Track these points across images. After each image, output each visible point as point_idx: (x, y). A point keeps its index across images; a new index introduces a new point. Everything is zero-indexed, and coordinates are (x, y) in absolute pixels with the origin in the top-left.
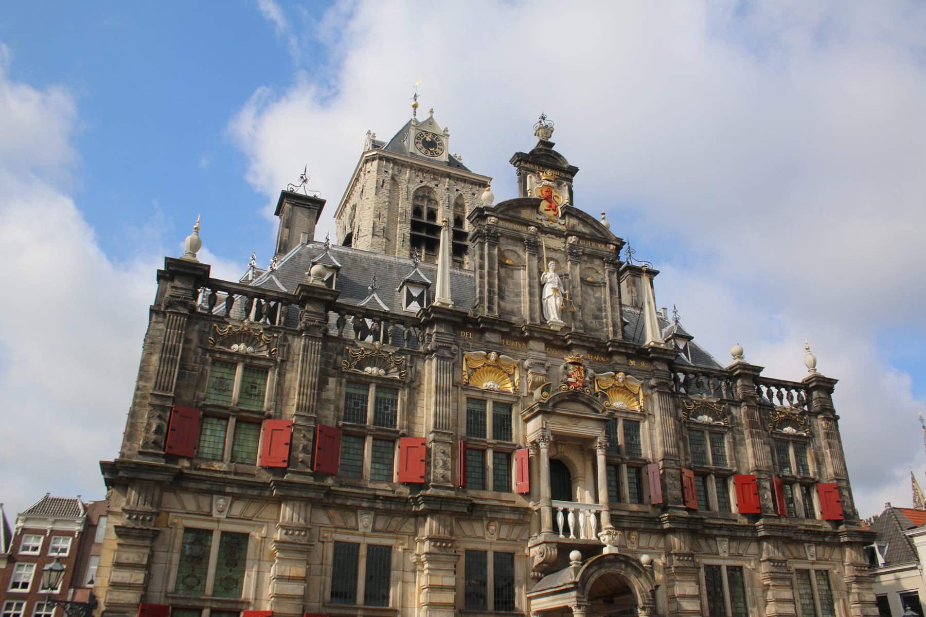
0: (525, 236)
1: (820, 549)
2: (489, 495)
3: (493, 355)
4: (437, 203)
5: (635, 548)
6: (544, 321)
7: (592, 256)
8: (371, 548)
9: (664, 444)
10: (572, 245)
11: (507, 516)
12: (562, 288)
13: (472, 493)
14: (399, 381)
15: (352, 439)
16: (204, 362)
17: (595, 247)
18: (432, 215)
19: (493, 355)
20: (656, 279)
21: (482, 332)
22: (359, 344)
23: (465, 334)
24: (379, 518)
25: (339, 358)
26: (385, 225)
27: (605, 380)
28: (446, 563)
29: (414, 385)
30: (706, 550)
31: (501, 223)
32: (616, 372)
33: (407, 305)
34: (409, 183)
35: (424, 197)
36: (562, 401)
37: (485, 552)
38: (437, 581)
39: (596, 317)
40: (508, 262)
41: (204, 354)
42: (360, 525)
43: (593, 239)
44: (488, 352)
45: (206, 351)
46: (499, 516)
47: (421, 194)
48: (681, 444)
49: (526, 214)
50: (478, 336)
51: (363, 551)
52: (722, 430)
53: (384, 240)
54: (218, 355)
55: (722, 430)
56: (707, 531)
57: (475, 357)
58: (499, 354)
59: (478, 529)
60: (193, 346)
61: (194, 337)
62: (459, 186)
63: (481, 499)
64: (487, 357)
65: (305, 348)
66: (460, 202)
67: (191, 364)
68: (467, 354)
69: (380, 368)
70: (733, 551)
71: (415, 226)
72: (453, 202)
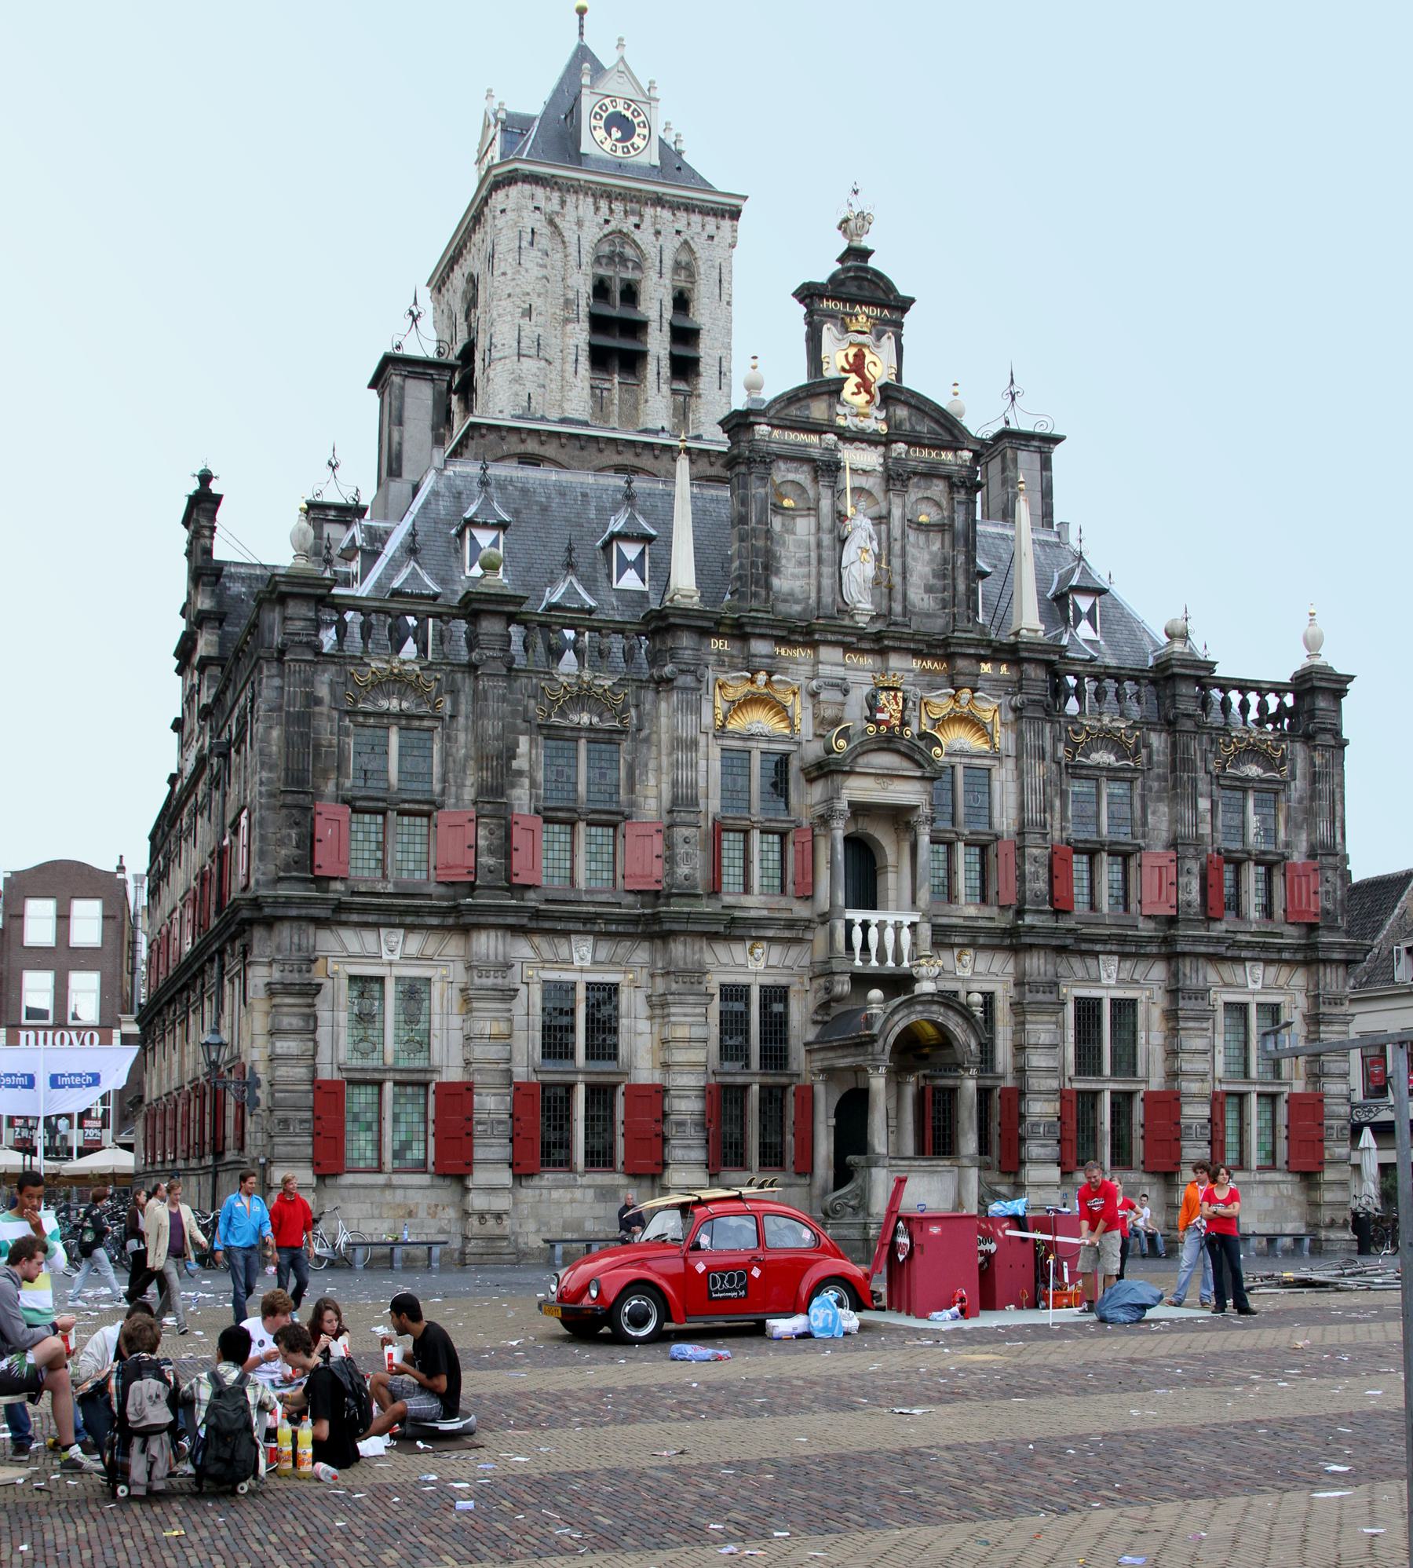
1: (1272, 970)
2: (756, 904)
3: (762, 677)
4: (638, 266)
6: (846, 610)
8: (590, 986)
15: (557, 827)
18: (630, 294)
19: (762, 677)
24: (600, 944)
29: (643, 734)
30: (1081, 973)
37: (748, 987)
42: (576, 957)
47: (606, 249)
51: (581, 993)
56: (1084, 946)
58: (770, 674)
59: (738, 952)
64: (752, 681)
66: (684, 258)
71: (598, 323)
72: (668, 263)
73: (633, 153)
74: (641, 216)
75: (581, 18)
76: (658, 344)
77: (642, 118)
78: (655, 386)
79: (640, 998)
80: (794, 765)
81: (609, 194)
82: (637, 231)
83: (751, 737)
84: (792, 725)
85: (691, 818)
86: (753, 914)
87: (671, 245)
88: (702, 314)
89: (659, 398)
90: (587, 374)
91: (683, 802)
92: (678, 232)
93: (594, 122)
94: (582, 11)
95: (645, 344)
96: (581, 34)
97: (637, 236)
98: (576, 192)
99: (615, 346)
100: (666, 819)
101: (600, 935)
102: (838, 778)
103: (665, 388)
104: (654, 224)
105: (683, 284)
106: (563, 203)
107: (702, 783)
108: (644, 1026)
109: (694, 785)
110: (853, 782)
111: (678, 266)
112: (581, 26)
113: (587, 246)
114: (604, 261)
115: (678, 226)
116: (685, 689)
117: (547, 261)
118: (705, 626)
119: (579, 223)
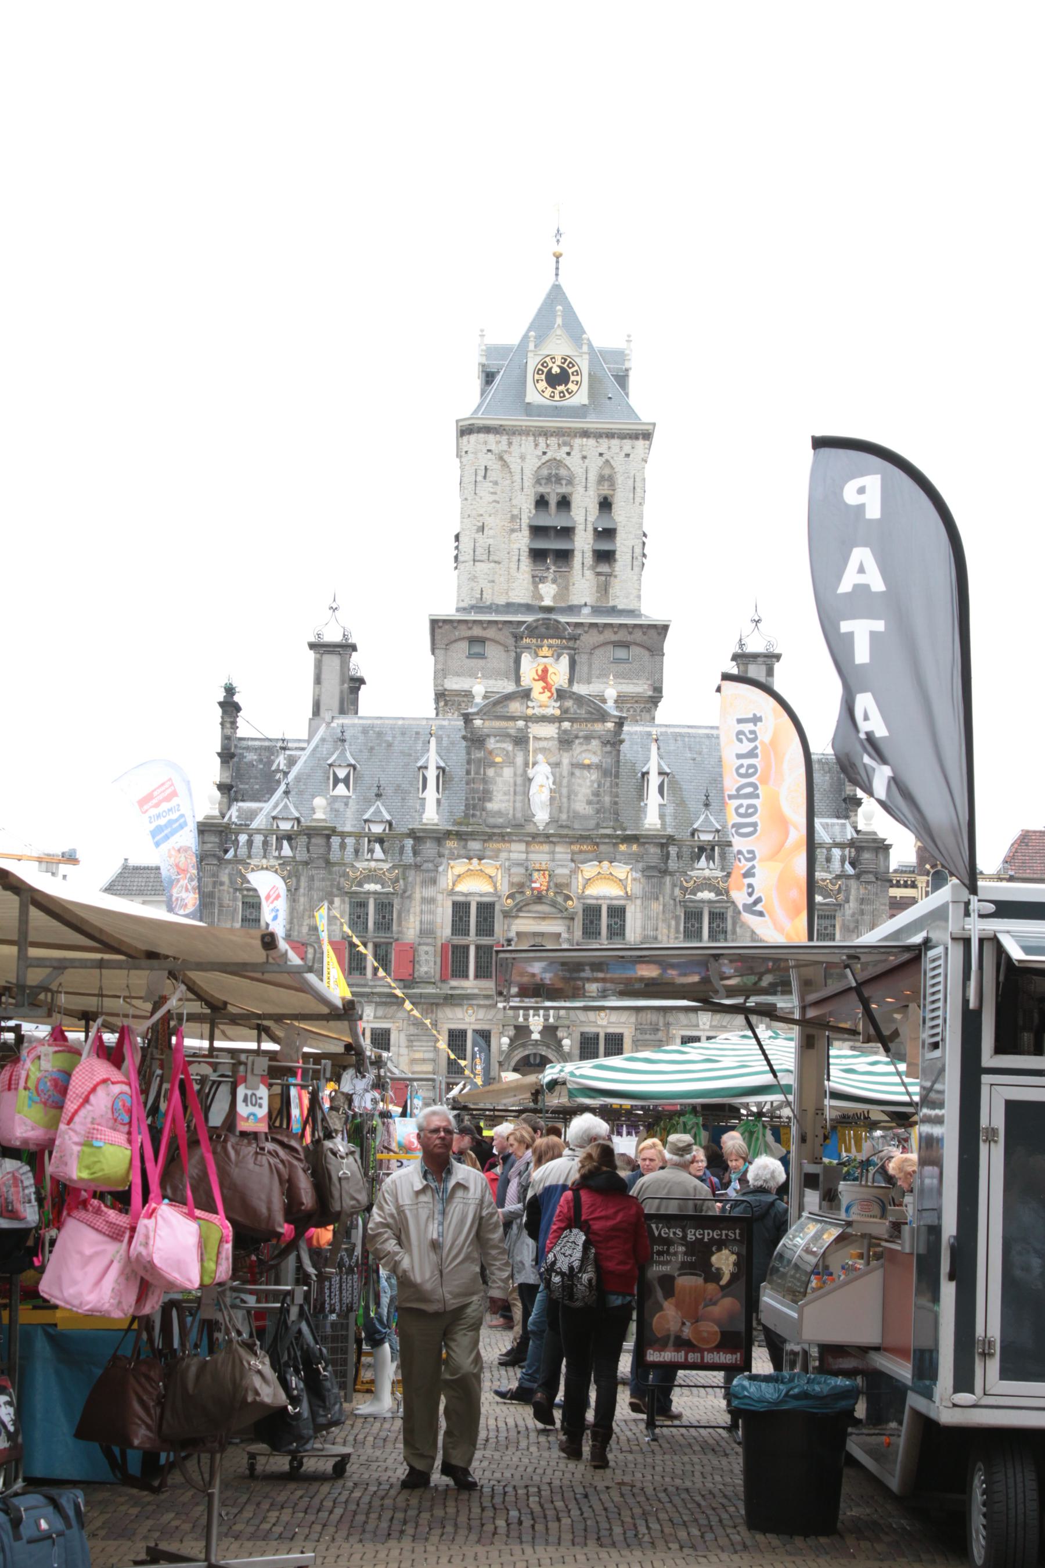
0: (512, 732)
4: (570, 482)
5: (605, 1023)
6: (529, 818)
7: (588, 738)
8: (372, 1029)
9: (644, 928)
10: (565, 731)
11: (482, 1002)
12: (551, 781)
13: (454, 983)
14: (393, 894)
16: (235, 899)
17: (592, 728)
18: (564, 503)
20: (777, 667)
21: (466, 840)
22: (357, 865)
23: (451, 844)
25: (342, 879)
26: (491, 541)
27: (589, 870)
28: (427, 1041)
29: (407, 894)
31: (488, 723)
32: (600, 862)
33: (423, 791)
34: (528, 457)
35: (548, 479)
36: (527, 905)
38: (418, 1056)
39: (589, 803)
40: (498, 760)
41: (234, 893)
43: (586, 720)
44: (470, 858)
45: (236, 890)
46: (475, 1002)
47: (545, 472)
48: (673, 923)
49: (515, 707)
50: (462, 843)
52: (724, 905)
53: (493, 564)
54: (245, 893)
55: (724, 905)
57: (460, 866)
58: (480, 859)
60: (225, 888)
61: (225, 879)
62: (604, 442)
63: (463, 988)
65: (312, 879)
66: (607, 472)
67: (226, 902)
68: (452, 863)
69: (376, 883)
70: (714, 1023)
71: (537, 531)
72: (593, 477)
73: (567, 396)
74: (571, 446)
75: (557, 262)
76: (583, 543)
77: (576, 368)
78: (580, 572)
79: (403, 1036)
80: (497, 908)
81: (546, 433)
82: (568, 458)
83: (470, 894)
84: (495, 886)
85: (430, 940)
86: (469, 991)
87: (595, 465)
88: (620, 514)
89: (584, 581)
90: (528, 569)
91: (427, 932)
92: (601, 455)
93: (537, 377)
94: (558, 256)
95: (572, 541)
96: (557, 275)
97: (568, 460)
98: (520, 434)
99: (550, 548)
100: (417, 940)
101: (378, 1004)
102: (511, 920)
103: (589, 574)
104: (581, 451)
105: (606, 492)
106: (510, 444)
107: (439, 920)
108: (404, 1051)
109: (432, 923)
110: (518, 921)
111: (602, 479)
112: (557, 269)
113: (529, 474)
114: (543, 482)
115: (601, 450)
116: (428, 871)
117: (498, 489)
118: (440, 837)
119: (523, 458)
